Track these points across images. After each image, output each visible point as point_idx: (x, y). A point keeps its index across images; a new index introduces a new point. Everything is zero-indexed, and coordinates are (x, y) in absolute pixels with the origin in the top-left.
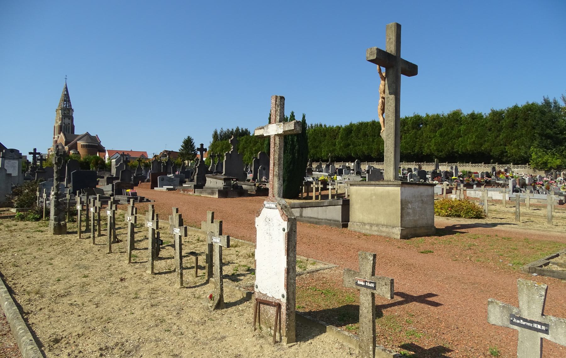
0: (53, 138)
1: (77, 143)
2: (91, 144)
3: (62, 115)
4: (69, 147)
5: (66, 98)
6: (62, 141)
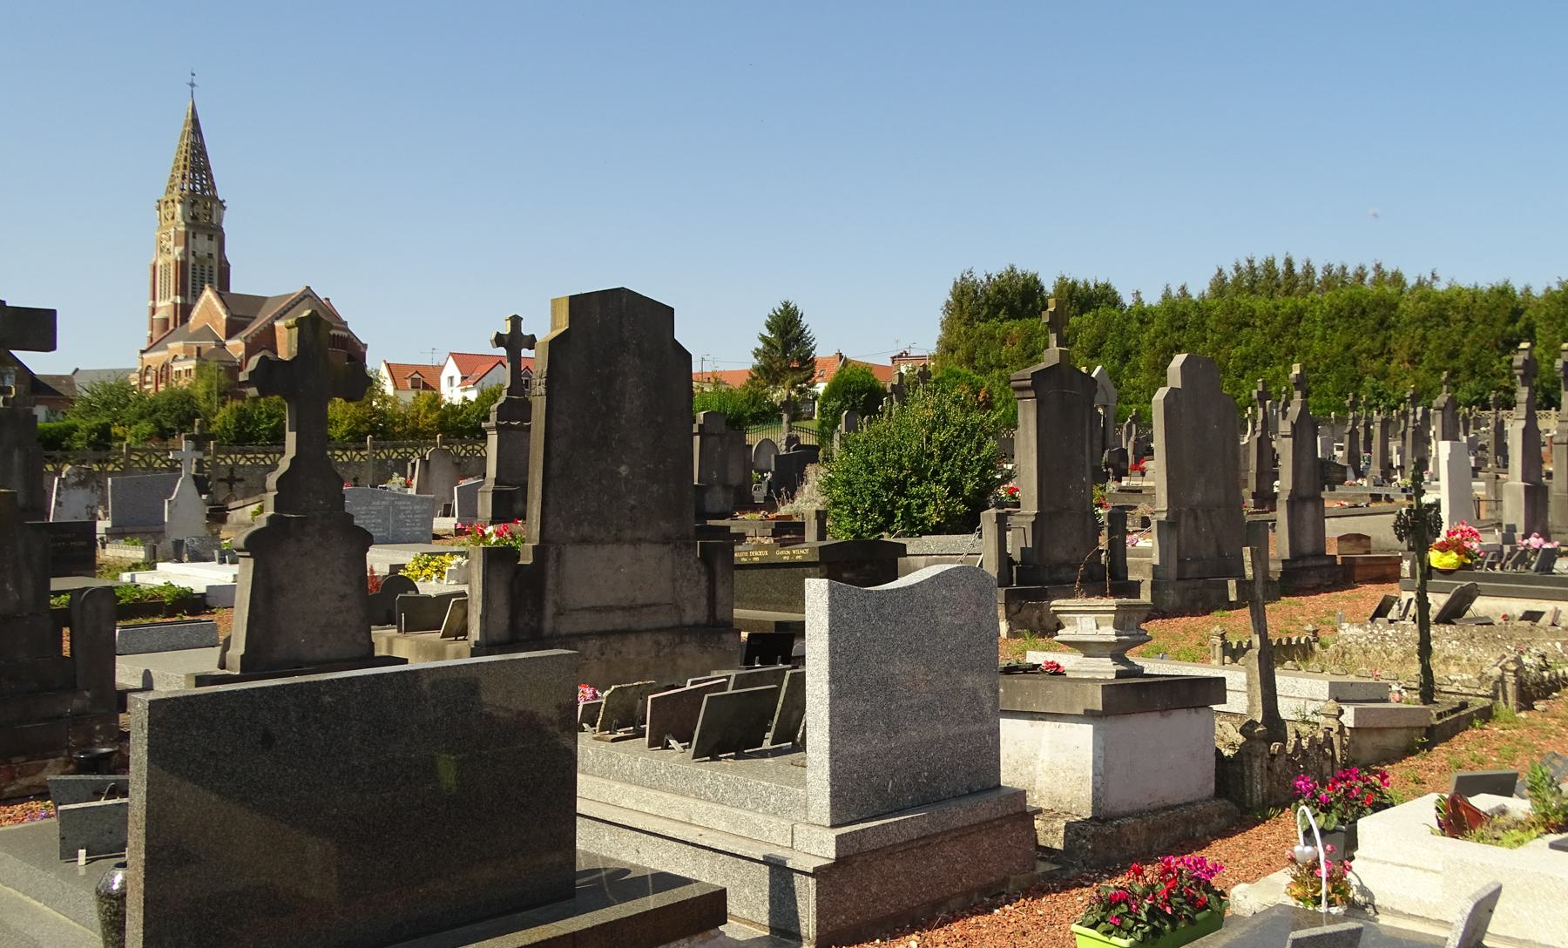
0: (148, 312)
1: (273, 327)
3: (187, 224)
4: (246, 344)
5: (197, 160)
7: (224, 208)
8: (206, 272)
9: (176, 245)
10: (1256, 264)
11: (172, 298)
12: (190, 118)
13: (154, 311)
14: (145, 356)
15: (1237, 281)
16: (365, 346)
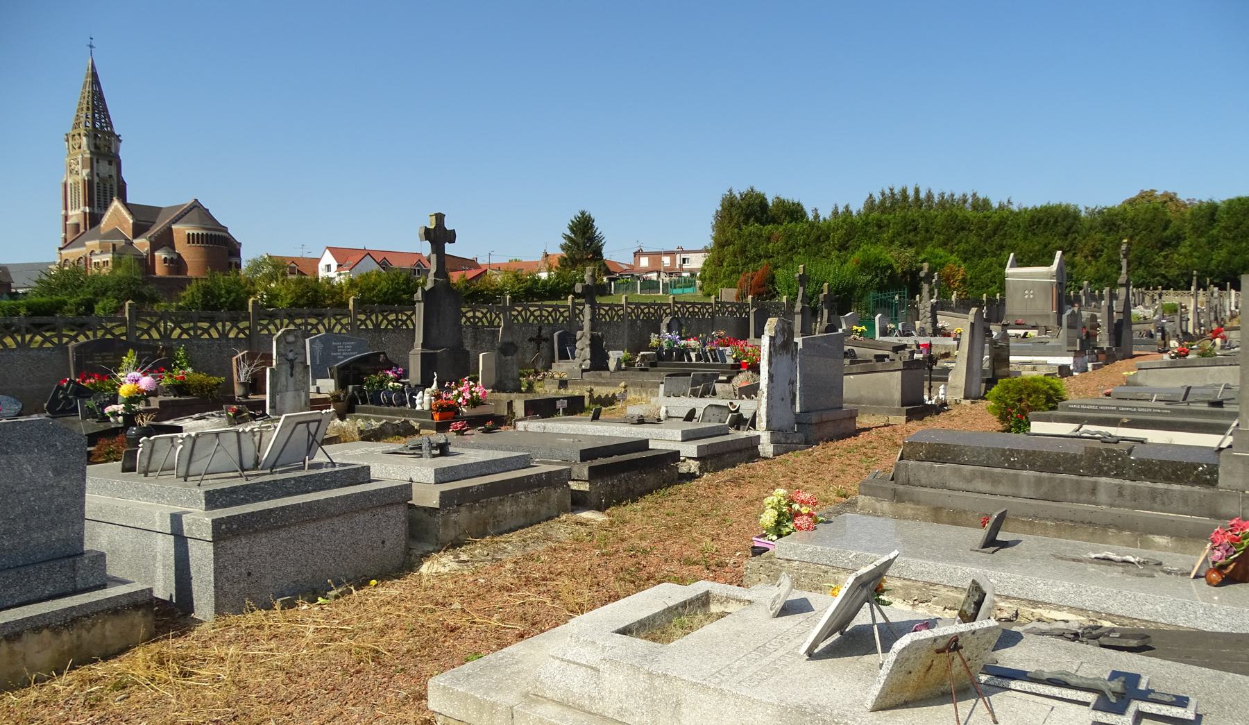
0: (61, 220)
1: (170, 229)
2: (213, 233)
3: (91, 153)
4: (151, 242)
5: (97, 103)
6: (120, 226)
7: (120, 141)
8: (108, 189)
9: (83, 168)
10: (896, 191)
11: (82, 208)
12: (90, 71)
13: (66, 218)
14: (63, 252)
15: (883, 203)
16: (240, 244)
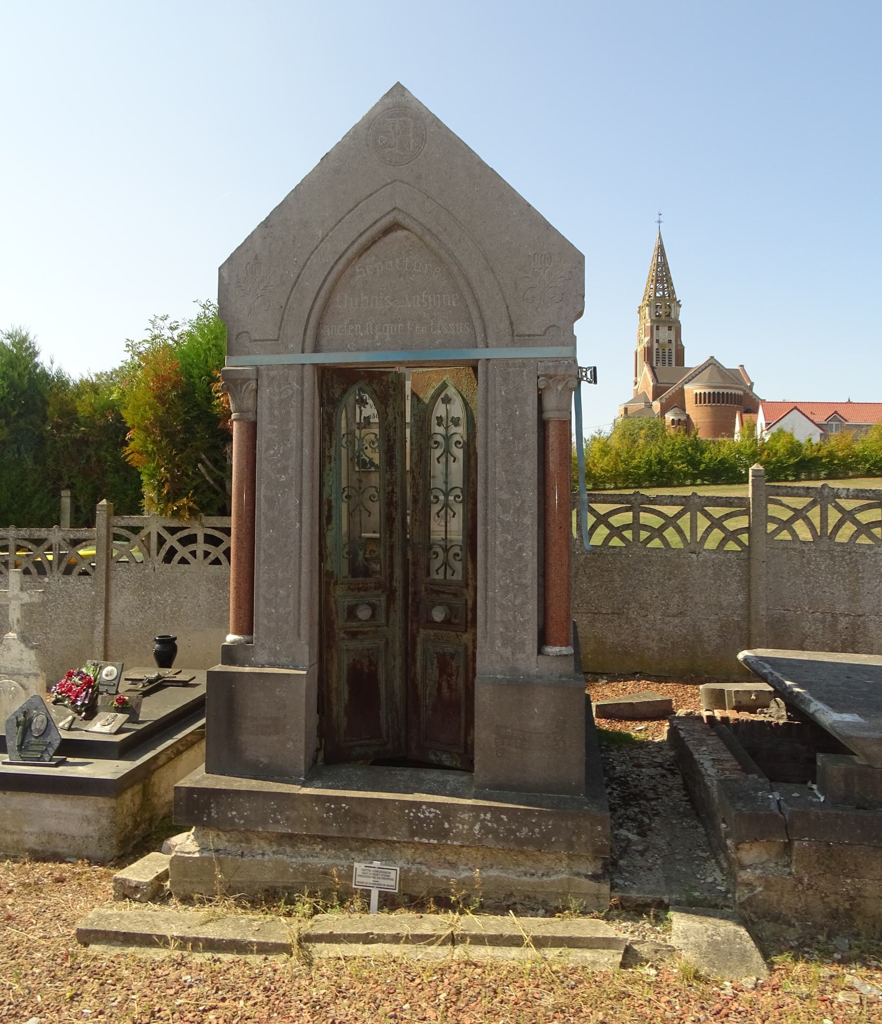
2: (721, 391)
3: (652, 321)
4: (661, 404)
6: (647, 389)
7: (680, 306)
8: (667, 354)
